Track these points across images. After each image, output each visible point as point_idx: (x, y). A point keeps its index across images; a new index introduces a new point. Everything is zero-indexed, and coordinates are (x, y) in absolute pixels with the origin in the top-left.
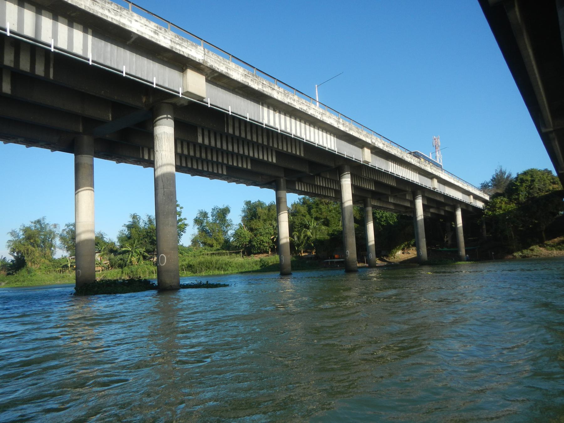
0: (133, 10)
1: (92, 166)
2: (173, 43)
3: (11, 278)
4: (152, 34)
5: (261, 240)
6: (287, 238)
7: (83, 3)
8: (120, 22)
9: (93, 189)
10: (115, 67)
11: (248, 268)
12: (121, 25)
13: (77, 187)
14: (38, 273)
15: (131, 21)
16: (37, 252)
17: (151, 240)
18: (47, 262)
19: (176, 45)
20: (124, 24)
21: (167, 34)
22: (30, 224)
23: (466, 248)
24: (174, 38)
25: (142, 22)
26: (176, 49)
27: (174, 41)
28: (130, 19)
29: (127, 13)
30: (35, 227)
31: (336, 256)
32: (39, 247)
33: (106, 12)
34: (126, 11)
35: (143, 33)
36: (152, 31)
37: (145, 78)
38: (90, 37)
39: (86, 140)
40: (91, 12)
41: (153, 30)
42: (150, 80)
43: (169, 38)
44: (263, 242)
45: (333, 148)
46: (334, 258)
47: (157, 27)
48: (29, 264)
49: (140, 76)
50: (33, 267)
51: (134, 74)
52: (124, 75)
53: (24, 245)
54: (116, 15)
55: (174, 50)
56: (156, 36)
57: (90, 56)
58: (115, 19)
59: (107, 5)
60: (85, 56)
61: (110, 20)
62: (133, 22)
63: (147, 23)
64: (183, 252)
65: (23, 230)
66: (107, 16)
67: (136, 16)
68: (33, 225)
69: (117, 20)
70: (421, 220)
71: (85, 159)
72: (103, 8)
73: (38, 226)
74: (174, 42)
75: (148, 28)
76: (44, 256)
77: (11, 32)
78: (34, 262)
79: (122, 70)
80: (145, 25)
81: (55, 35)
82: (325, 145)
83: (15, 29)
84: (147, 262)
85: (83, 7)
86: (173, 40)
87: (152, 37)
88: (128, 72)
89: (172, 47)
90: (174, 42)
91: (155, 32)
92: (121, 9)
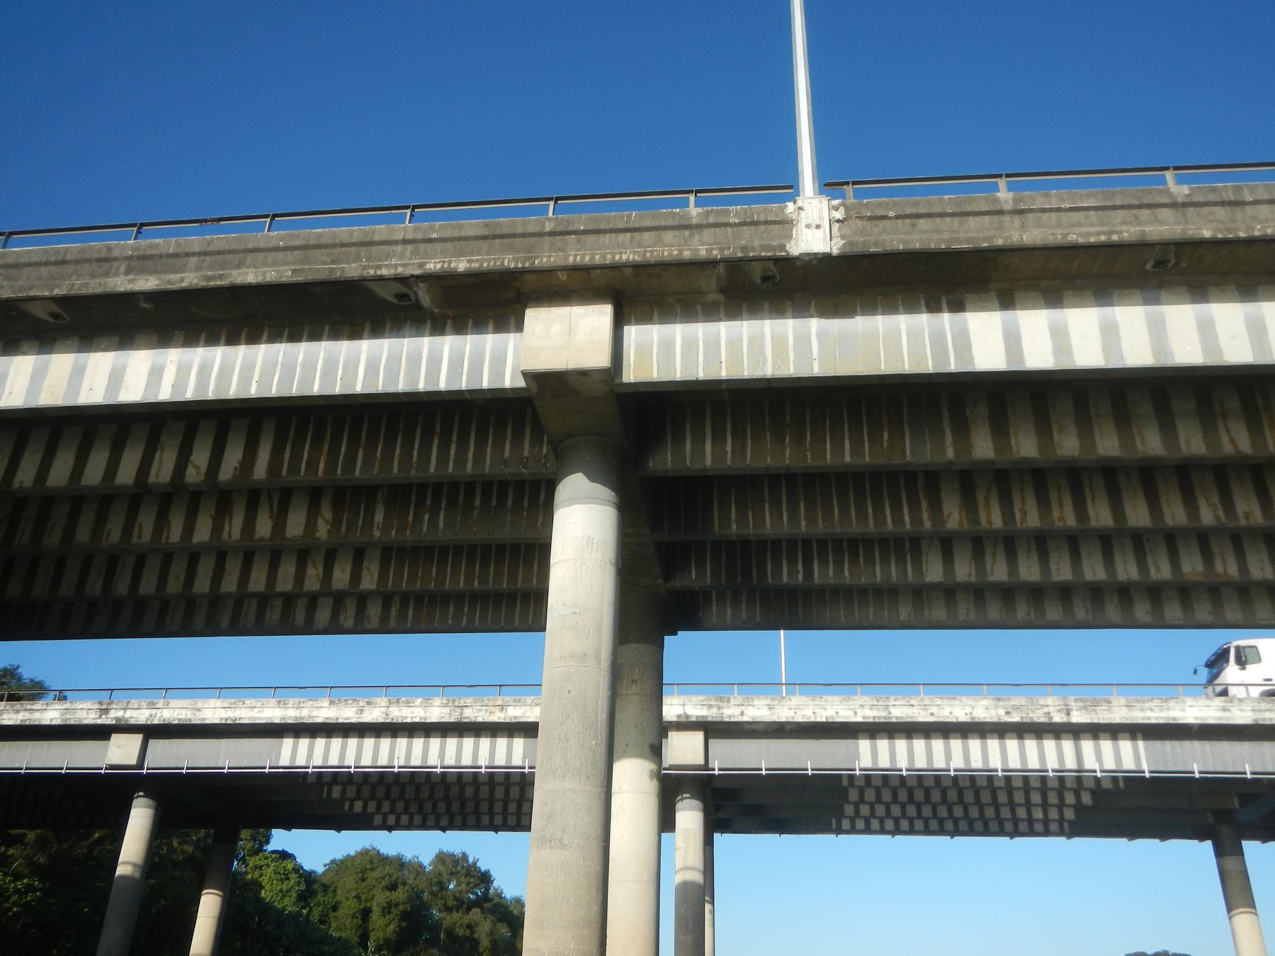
0: (1187, 695)
1: (1244, 874)
2: (1258, 713)
4: (1220, 714)
7: (1117, 715)
8: (1168, 718)
9: (1253, 911)
10: (1182, 769)
12: (1171, 722)
13: (1230, 908)
15: (1184, 710)
19: (1262, 713)
20: (1174, 719)
21: (1243, 704)
24: (1257, 705)
25: (1201, 704)
26: (1264, 719)
27: (1259, 708)
28: (1182, 708)
29: (1176, 702)
33: (1149, 714)
34: (1174, 700)
35: (1203, 719)
36: (1218, 710)
37: (1232, 770)
38: (1141, 744)
39: (1224, 830)
40: (1129, 722)
41: (1219, 708)
42: (1240, 770)
43: (1249, 708)
47: (1225, 701)
49: (1221, 769)
51: (1212, 769)
52: (1197, 775)
54: (1161, 711)
55: (1261, 722)
56: (1227, 714)
57: (1145, 767)
58: (1160, 718)
59: (1147, 705)
60: (1139, 769)
61: (1154, 721)
62: (1188, 709)
63: (1208, 702)
66: (1149, 718)
67: (1189, 701)
69: (1163, 718)
71: (1231, 862)
72: (1143, 710)
74: (1259, 711)
75: (1211, 708)
77: (1054, 771)
79: (1192, 770)
80: (1207, 706)
83: (1057, 767)
85: (1118, 721)
86: (1255, 708)
87: (1220, 718)
88: (1203, 770)
89: (1256, 720)
90: (1259, 711)
91: (1225, 709)
92: (1166, 700)
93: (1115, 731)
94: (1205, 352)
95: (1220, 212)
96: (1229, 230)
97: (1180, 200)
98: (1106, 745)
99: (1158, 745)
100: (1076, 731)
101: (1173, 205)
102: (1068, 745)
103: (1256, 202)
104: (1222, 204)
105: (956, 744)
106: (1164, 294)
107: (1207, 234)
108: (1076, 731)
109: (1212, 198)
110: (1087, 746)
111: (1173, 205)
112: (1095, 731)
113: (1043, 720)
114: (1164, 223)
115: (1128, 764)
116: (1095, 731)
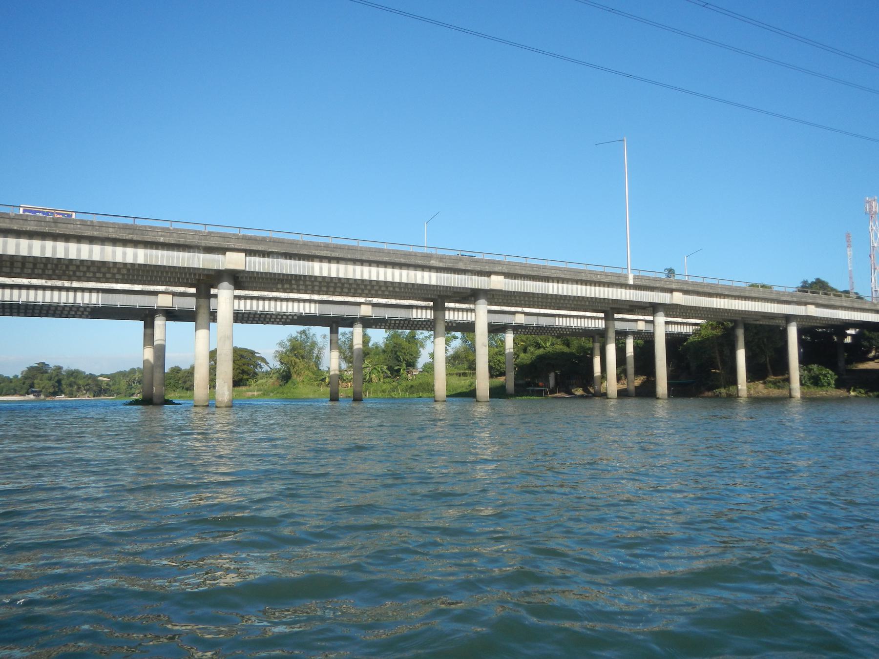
3: (281, 390)
5: (499, 361)
6: (335, 370)
11: (459, 391)
14: (301, 386)
16: (301, 364)
17: (395, 356)
18: (310, 374)
22: (296, 334)
23: (671, 381)
30: (301, 337)
31: (540, 384)
32: (304, 358)
38: (100, 294)
44: (500, 363)
45: (313, 311)
46: (538, 386)
48: (294, 376)
50: (298, 380)
53: (289, 356)
57: (100, 303)
64: (429, 370)
65: (290, 340)
68: (299, 335)
70: (509, 353)
71: (149, 331)
73: (303, 336)
76: (308, 369)
78: (298, 374)
81: (83, 299)
82: (302, 311)
83: (65, 302)
84: (387, 380)
93: (91, 290)
94: (16, 252)
95: (21, 221)
96: (22, 228)
97: (12, 217)
98: (87, 295)
99: (107, 295)
100: (76, 290)
101: (10, 218)
102: (71, 294)
103: (31, 220)
104: (22, 220)
105: (24, 292)
106: (9, 236)
107: (15, 228)
108: (76, 290)
109: (20, 218)
110: (79, 294)
111: (10, 218)
112: (83, 290)
113: (60, 285)
114: (6, 223)
115: (94, 301)
116: (83, 290)
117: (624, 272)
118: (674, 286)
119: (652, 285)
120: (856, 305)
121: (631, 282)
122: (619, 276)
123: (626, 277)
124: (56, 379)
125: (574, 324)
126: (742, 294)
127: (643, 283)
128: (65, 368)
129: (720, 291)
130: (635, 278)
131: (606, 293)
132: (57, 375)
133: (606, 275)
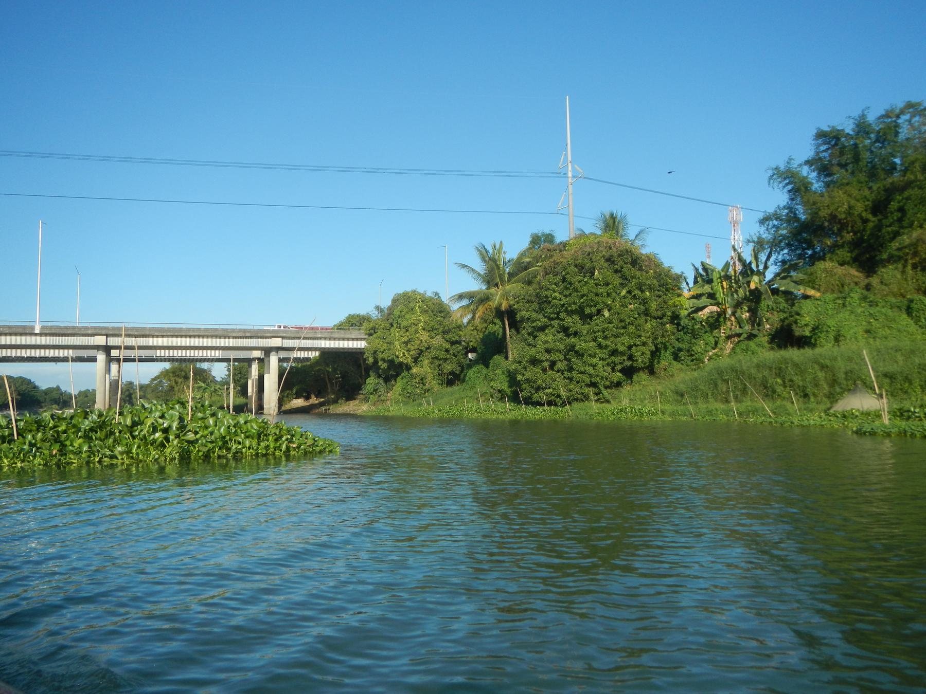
117: (31, 324)
118: (90, 332)
119: (62, 332)
120: (336, 336)
121: (37, 331)
122: (24, 327)
123: (33, 328)
124: (127, 393)
125: (178, 354)
126: (176, 334)
127: (53, 331)
128: (136, 383)
129: (147, 333)
130: (43, 328)
131: (48, 341)
132: (128, 390)
133: (10, 327)
